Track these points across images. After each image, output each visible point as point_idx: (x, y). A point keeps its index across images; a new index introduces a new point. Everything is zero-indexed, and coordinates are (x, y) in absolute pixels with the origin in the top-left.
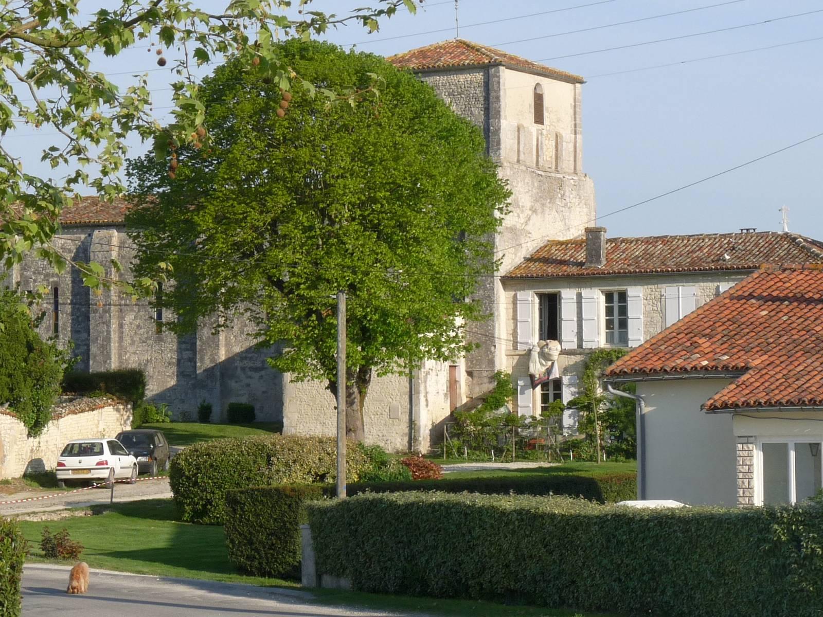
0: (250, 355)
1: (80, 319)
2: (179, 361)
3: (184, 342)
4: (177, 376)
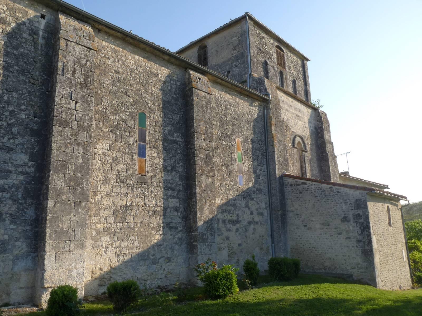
0: (229, 208)
1: (15, 130)
2: (165, 209)
3: (171, 189)
4: (163, 228)
